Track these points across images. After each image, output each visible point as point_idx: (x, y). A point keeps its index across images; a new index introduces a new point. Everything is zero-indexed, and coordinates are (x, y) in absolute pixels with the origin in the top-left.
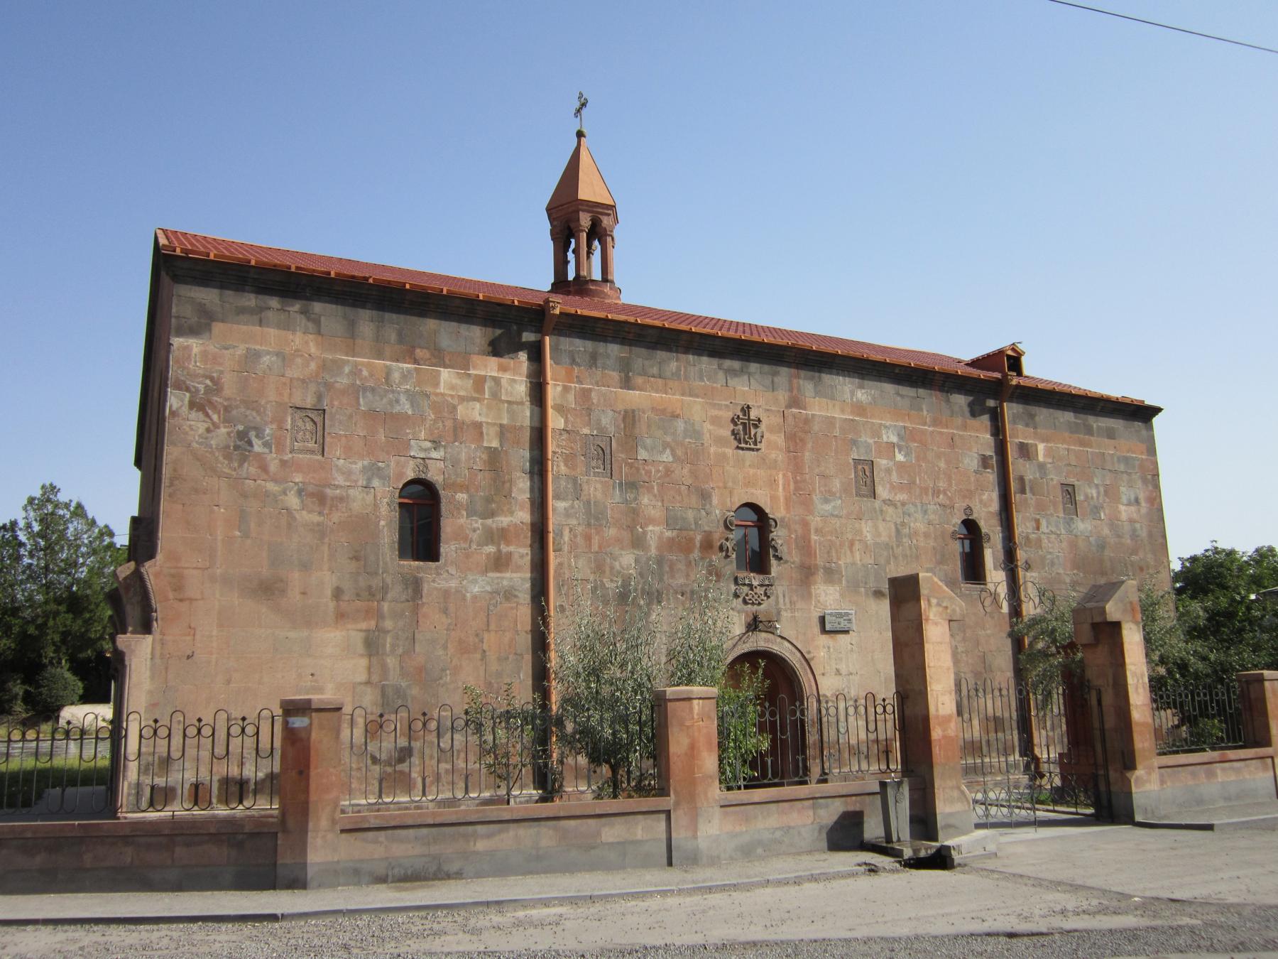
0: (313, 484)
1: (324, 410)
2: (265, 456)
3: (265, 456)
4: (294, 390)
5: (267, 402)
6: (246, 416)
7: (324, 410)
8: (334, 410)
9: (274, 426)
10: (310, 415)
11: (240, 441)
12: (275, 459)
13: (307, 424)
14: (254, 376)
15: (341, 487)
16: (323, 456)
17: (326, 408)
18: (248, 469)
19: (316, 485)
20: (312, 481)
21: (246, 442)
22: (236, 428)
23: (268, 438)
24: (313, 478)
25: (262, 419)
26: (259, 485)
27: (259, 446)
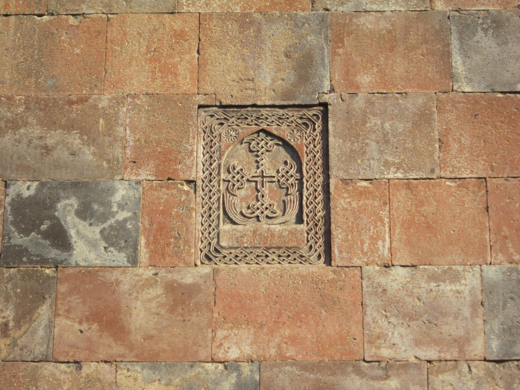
0: (295, 363)
1: (325, 105)
2: (115, 275)
3: (115, 275)
4: (211, 52)
5: (119, 101)
6: (48, 150)
7: (325, 105)
8: (359, 102)
9: (145, 174)
10: (273, 129)
11: (26, 232)
12: (150, 283)
13: (265, 161)
14: (72, 20)
15: (405, 366)
16: (329, 261)
17: (326, 98)
18: (50, 326)
19: (304, 367)
20: (291, 352)
21: (46, 235)
22: (12, 191)
23: (122, 215)
24: (293, 340)
25: (101, 155)
26: (89, 379)
27: (92, 245)
